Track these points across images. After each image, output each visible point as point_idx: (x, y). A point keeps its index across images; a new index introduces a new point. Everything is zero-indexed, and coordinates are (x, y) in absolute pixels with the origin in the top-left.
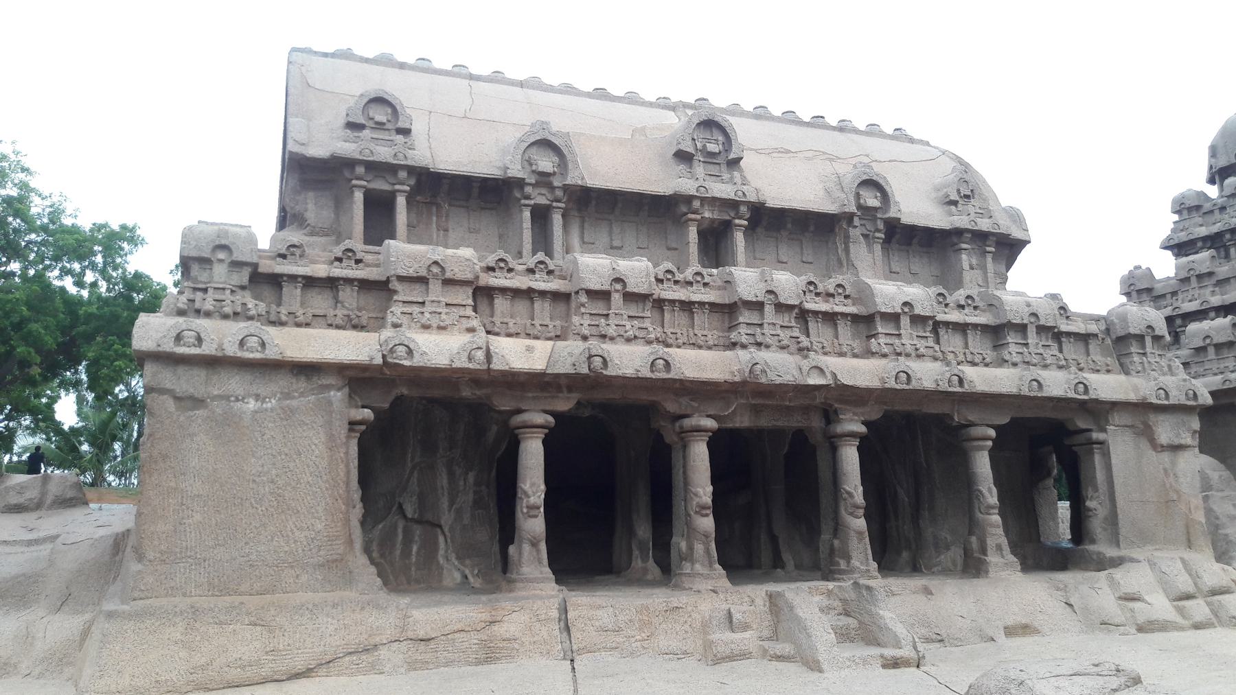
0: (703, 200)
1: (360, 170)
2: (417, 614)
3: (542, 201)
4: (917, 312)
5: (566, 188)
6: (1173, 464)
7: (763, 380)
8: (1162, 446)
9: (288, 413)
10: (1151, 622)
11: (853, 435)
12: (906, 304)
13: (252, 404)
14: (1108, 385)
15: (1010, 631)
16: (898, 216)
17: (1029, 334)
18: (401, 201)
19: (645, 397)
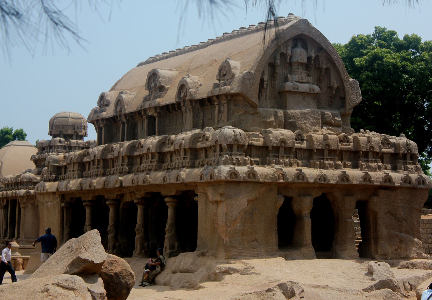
0: (145, 110)
7: (107, 187)
13: (49, 204)
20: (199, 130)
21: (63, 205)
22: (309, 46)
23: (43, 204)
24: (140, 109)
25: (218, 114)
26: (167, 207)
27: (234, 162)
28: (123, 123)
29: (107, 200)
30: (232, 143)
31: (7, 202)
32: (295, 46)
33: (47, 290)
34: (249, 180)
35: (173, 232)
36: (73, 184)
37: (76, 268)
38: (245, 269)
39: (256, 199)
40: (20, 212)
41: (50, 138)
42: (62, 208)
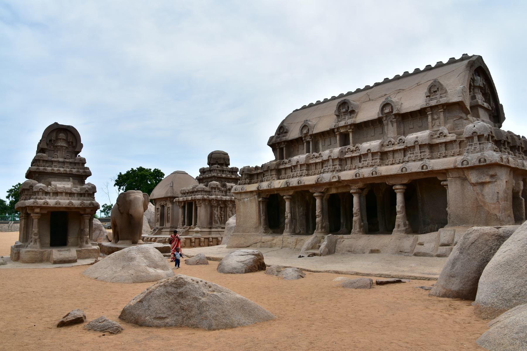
0: (338, 128)
1: (277, 145)
2: (263, 237)
3: (308, 139)
4: (372, 151)
5: (311, 135)
6: (482, 191)
7: (321, 182)
8: (473, 184)
9: (251, 200)
10: (419, 253)
11: (355, 193)
12: (369, 150)
13: (246, 200)
15: (372, 251)
16: (396, 112)
17: (416, 149)
18: (284, 149)
19: (306, 189)
21: (260, 199)
24: (333, 127)
28: (308, 143)
29: (283, 196)
31: (185, 204)
41: (208, 166)
42: (259, 202)
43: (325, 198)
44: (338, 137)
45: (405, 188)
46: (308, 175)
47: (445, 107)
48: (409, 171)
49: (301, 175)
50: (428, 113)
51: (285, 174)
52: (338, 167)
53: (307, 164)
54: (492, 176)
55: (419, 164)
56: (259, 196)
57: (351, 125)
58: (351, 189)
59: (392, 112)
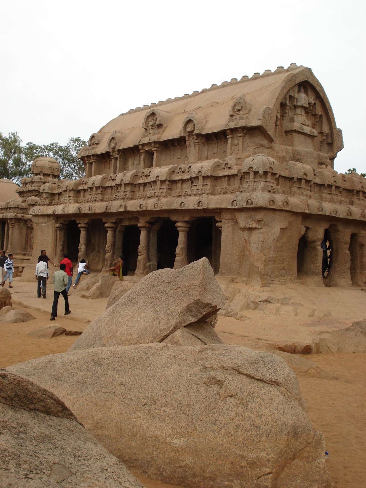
0: (143, 145)
1: (86, 158)
3: (117, 156)
5: (119, 151)
7: (110, 211)
8: (241, 228)
11: (142, 227)
12: (158, 176)
14: (213, 202)
20: (218, 159)
21: (57, 225)
22: (310, 92)
23: (37, 224)
25: (231, 148)
26: (178, 232)
27: (270, 189)
30: (268, 170)
32: (299, 91)
33: (219, 383)
34: (284, 208)
35: (183, 256)
36: (70, 207)
37: (193, 316)
38: (285, 298)
39: (286, 228)
40: (8, 230)
43: (118, 229)
44: (143, 156)
45: (190, 226)
46: (102, 200)
47: (245, 132)
48: (186, 207)
49: (95, 200)
50: (228, 137)
51: (84, 196)
52: (129, 194)
53: (102, 187)
54: (259, 221)
55: (196, 199)
56: (57, 222)
57: (155, 143)
58: (139, 222)
59: (194, 131)
